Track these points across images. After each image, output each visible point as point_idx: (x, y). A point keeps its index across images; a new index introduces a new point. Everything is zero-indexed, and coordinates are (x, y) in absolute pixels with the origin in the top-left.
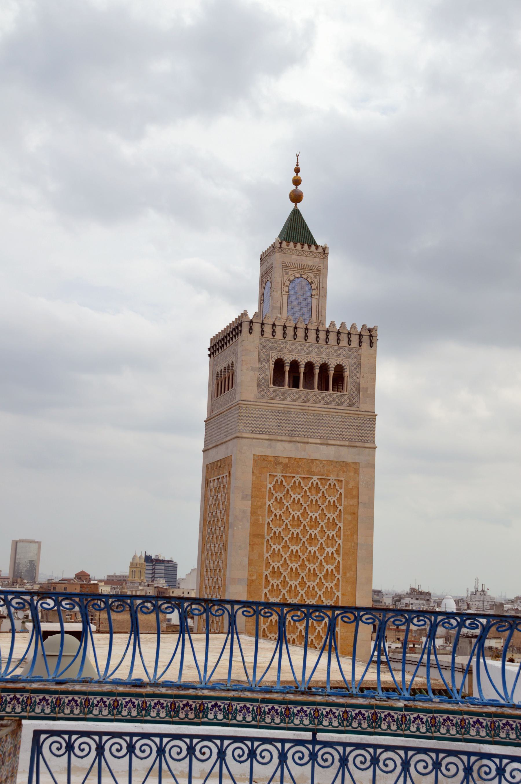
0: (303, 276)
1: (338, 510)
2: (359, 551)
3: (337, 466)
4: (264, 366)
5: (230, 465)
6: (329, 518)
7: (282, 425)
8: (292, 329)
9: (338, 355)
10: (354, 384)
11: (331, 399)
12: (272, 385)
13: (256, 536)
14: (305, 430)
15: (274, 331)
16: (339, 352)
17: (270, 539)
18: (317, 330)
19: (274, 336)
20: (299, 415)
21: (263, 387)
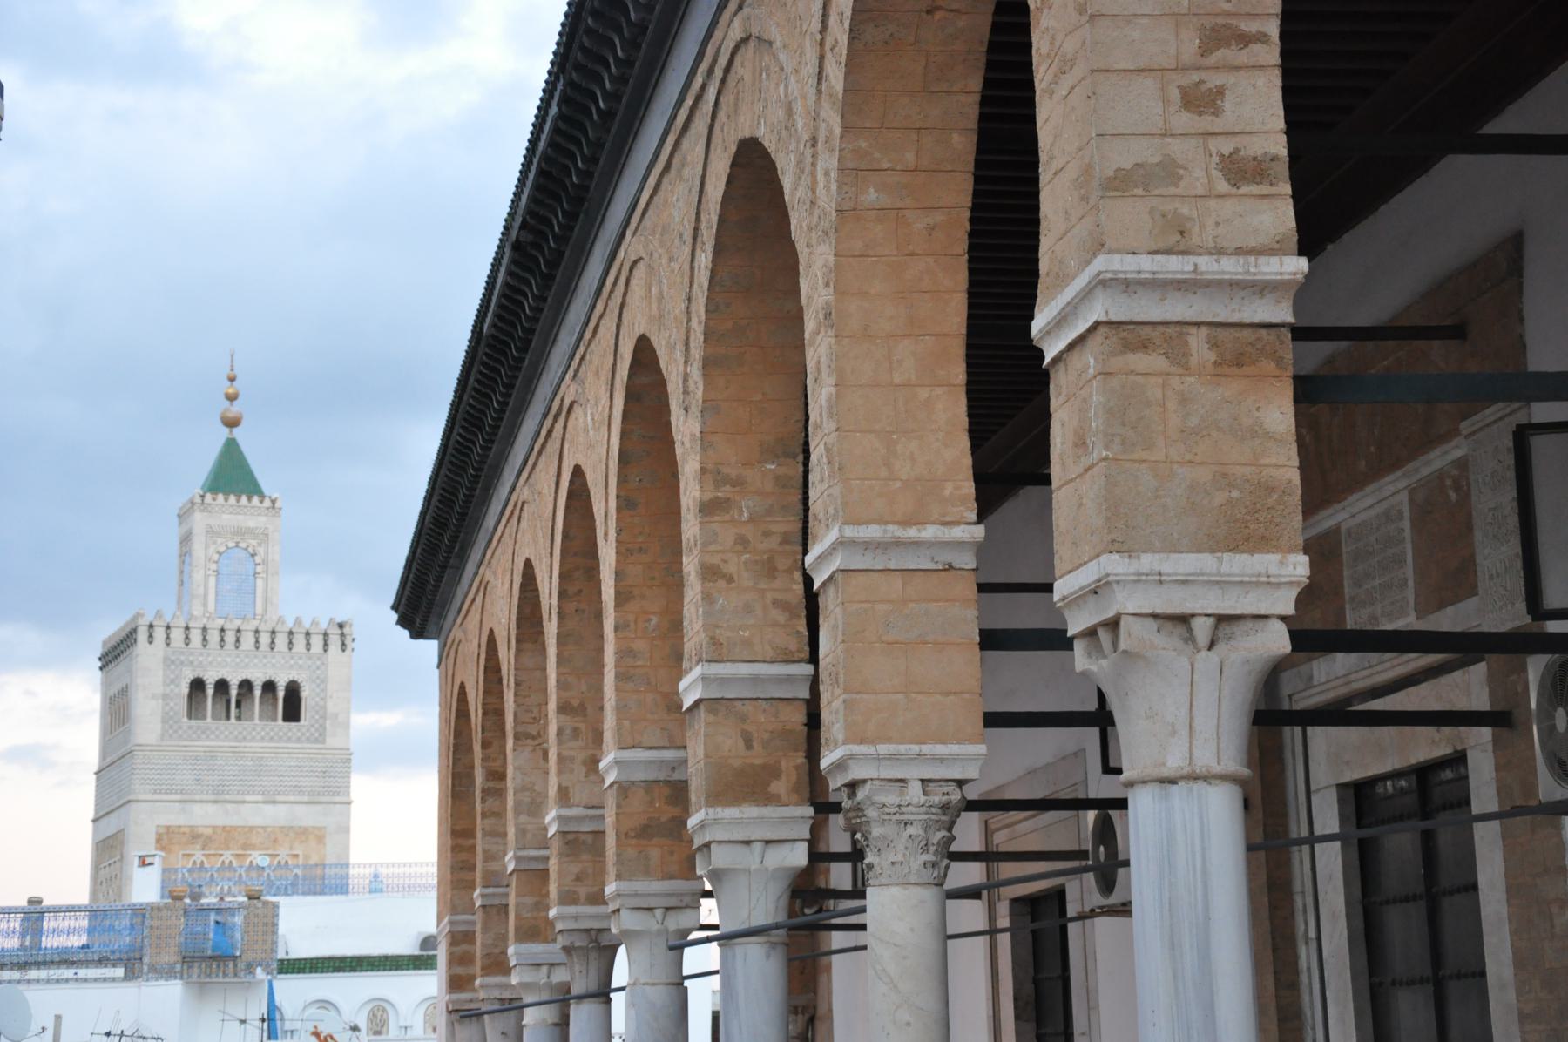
5: (122, 843)
9: (291, 667)
12: (185, 719)
15: (187, 638)
18: (257, 631)
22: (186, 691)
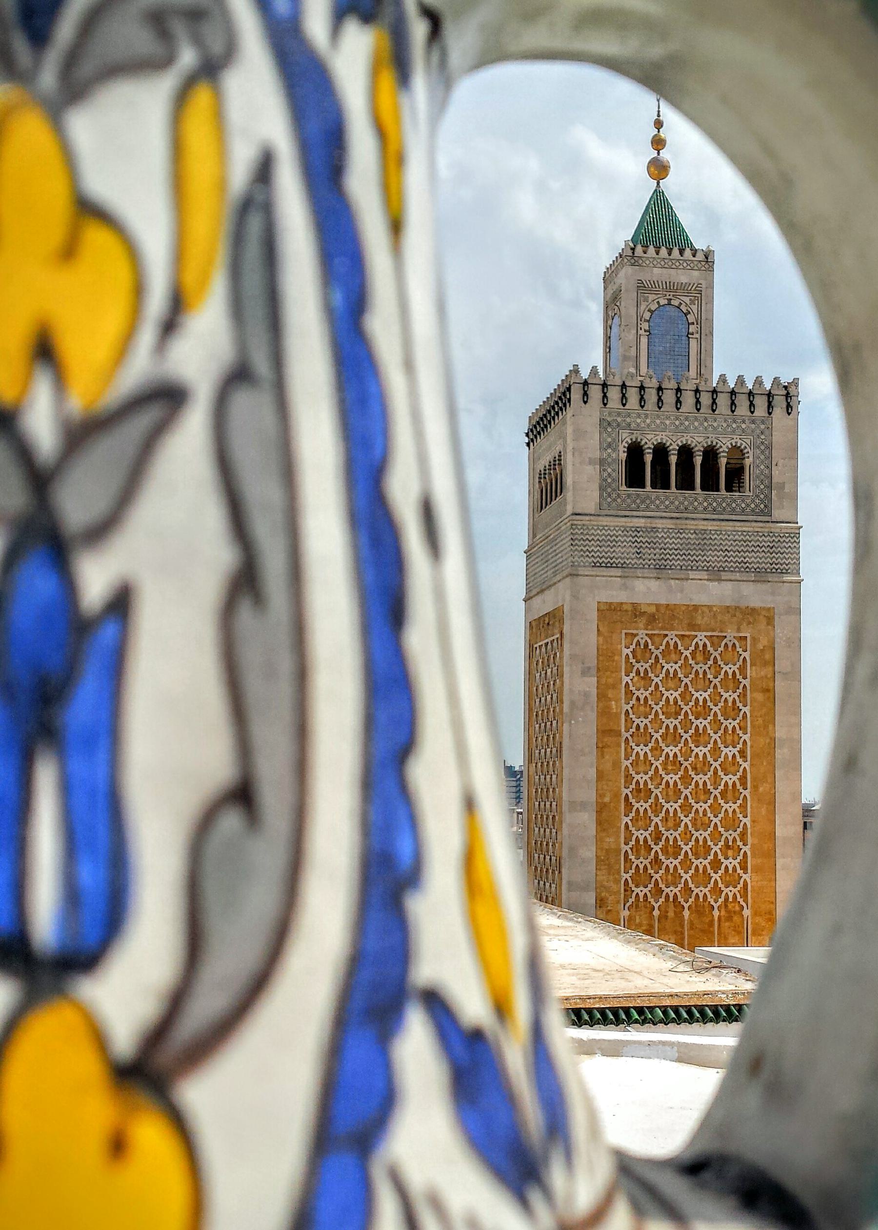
0: (673, 302)
1: (741, 686)
3: (738, 614)
4: (609, 455)
5: (561, 621)
6: (726, 700)
7: (644, 552)
8: (654, 392)
9: (734, 432)
10: (762, 477)
11: (724, 505)
12: (624, 488)
13: (607, 733)
14: (681, 558)
16: (734, 426)
17: (630, 738)
19: (624, 405)
20: (671, 533)
21: (609, 490)
22: (623, 456)
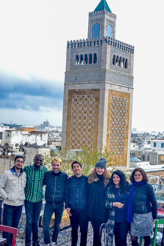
2: (99, 121)
16: (95, 49)
